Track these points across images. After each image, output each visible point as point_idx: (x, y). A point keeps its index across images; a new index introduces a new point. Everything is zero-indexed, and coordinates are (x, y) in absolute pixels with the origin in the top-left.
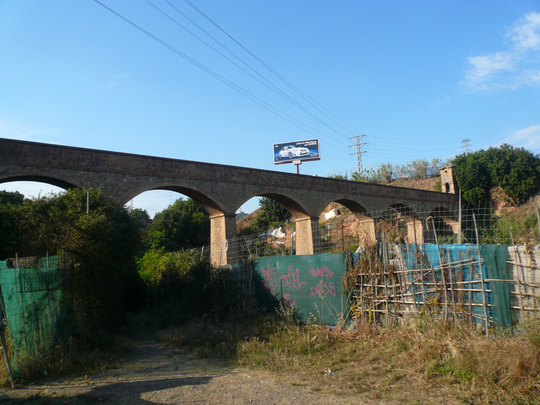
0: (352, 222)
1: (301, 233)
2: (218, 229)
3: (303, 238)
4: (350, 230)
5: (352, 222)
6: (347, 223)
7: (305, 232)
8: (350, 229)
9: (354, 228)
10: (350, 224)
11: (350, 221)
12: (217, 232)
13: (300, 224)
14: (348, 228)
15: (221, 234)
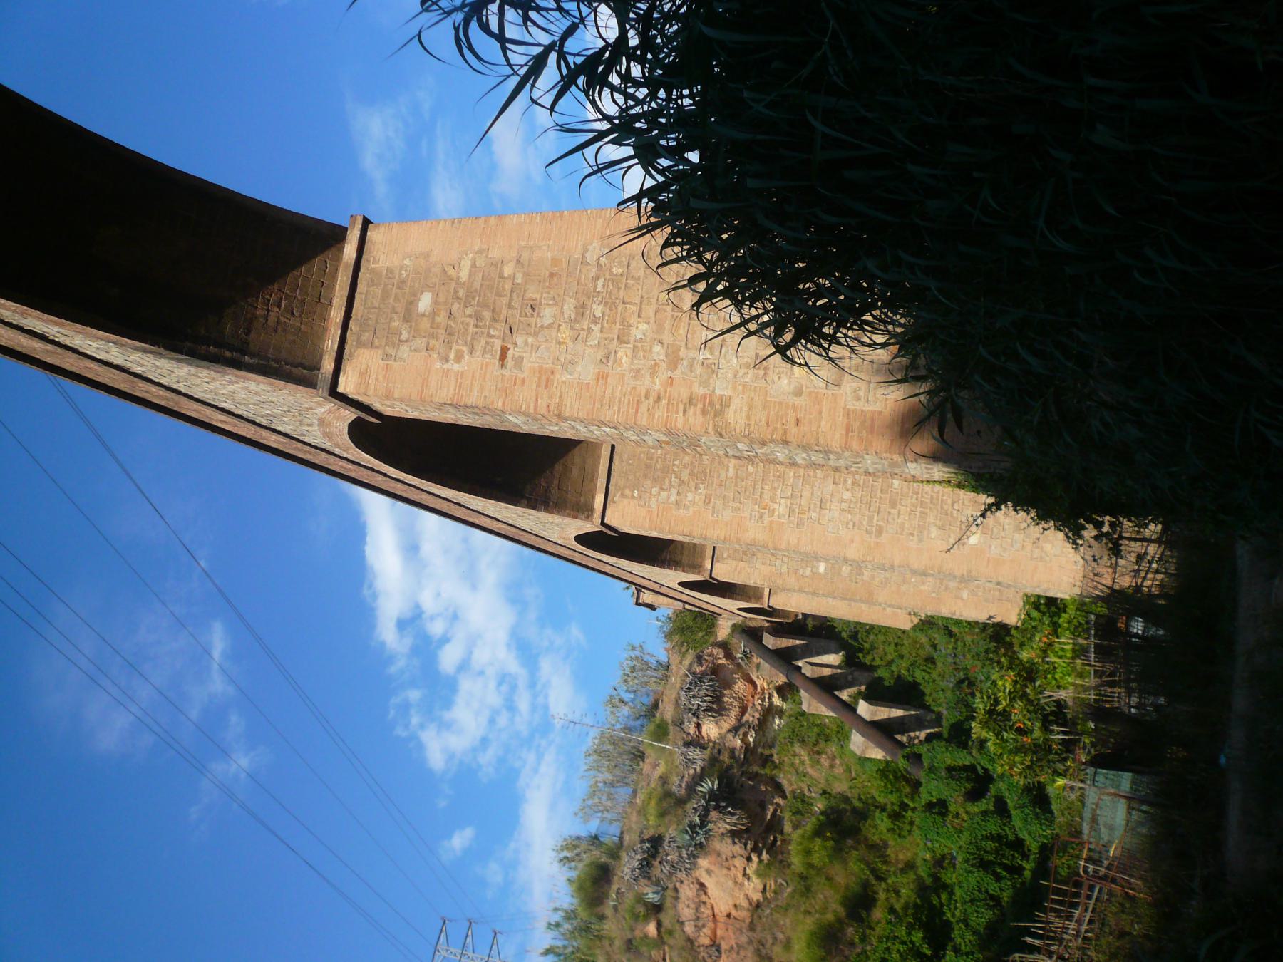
0: (704, 898)
1: (664, 494)
2: (425, 302)
3: (692, 484)
4: (734, 913)
5: (704, 898)
6: (704, 926)
7: (666, 470)
8: (729, 916)
9: (730, 883)
10: (709, 912)
11: (697, 909)
12: (441, 319)
13: (623, 496)
14: (721, 918)
15: (464, 275)
